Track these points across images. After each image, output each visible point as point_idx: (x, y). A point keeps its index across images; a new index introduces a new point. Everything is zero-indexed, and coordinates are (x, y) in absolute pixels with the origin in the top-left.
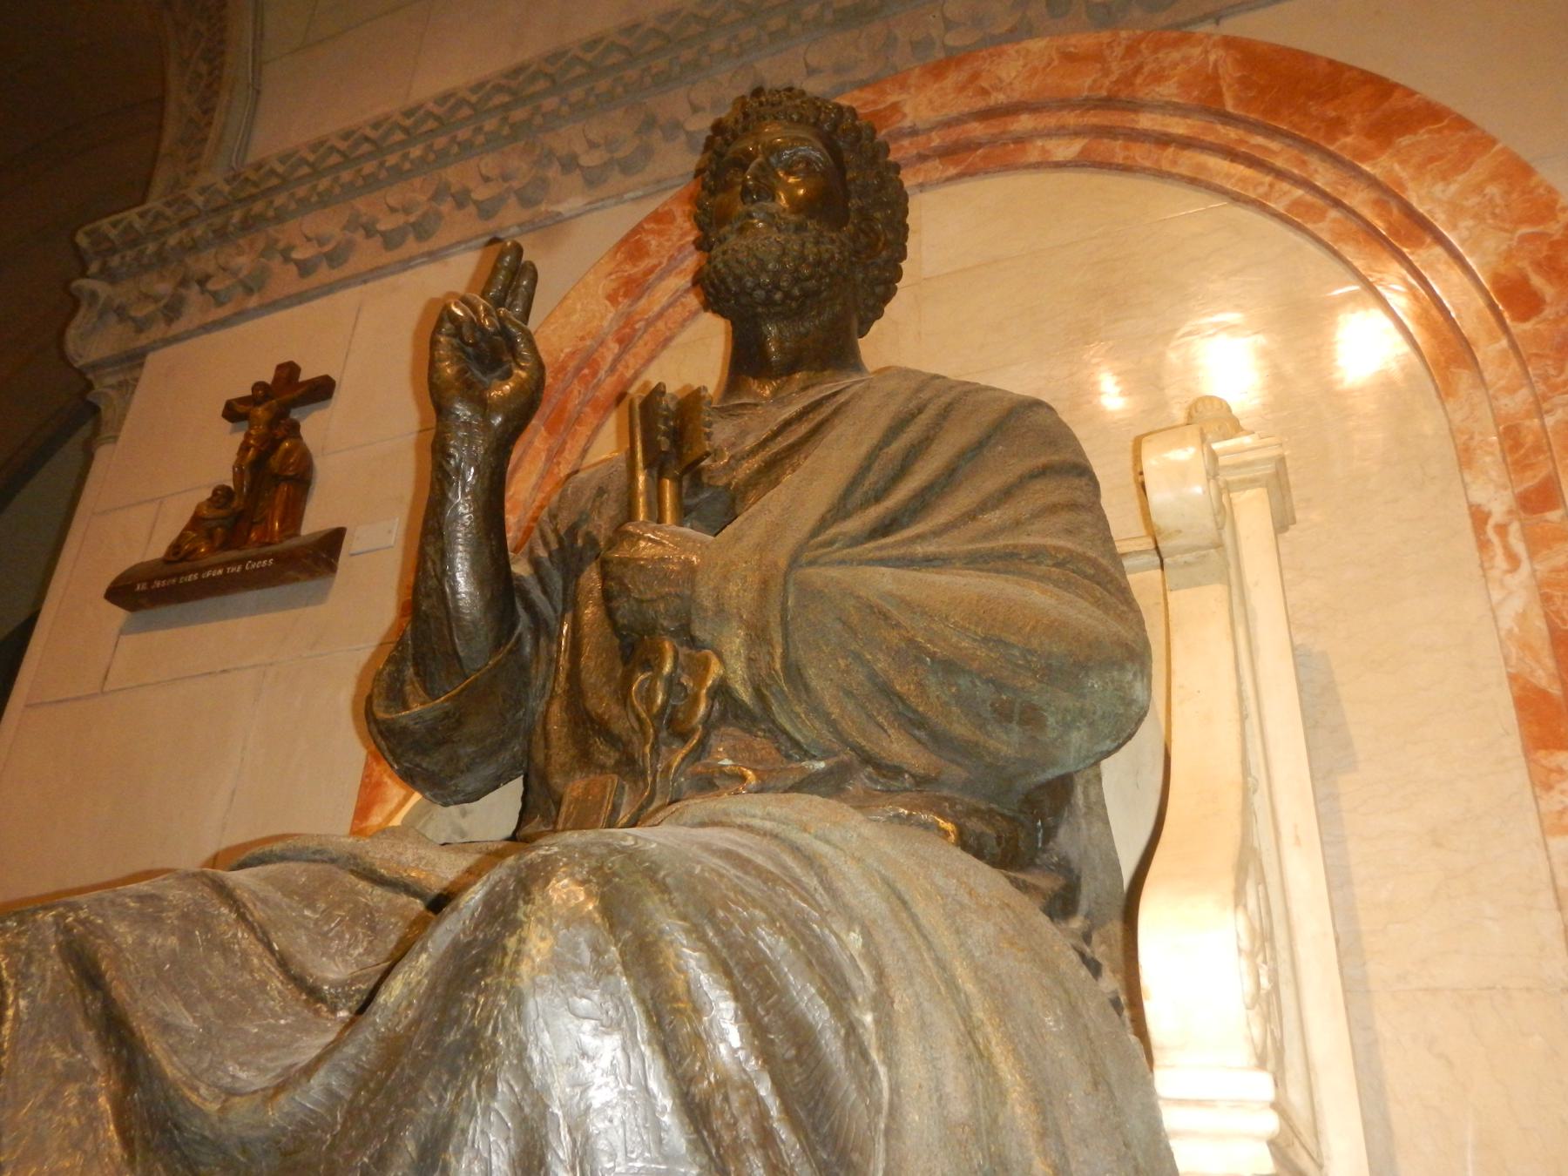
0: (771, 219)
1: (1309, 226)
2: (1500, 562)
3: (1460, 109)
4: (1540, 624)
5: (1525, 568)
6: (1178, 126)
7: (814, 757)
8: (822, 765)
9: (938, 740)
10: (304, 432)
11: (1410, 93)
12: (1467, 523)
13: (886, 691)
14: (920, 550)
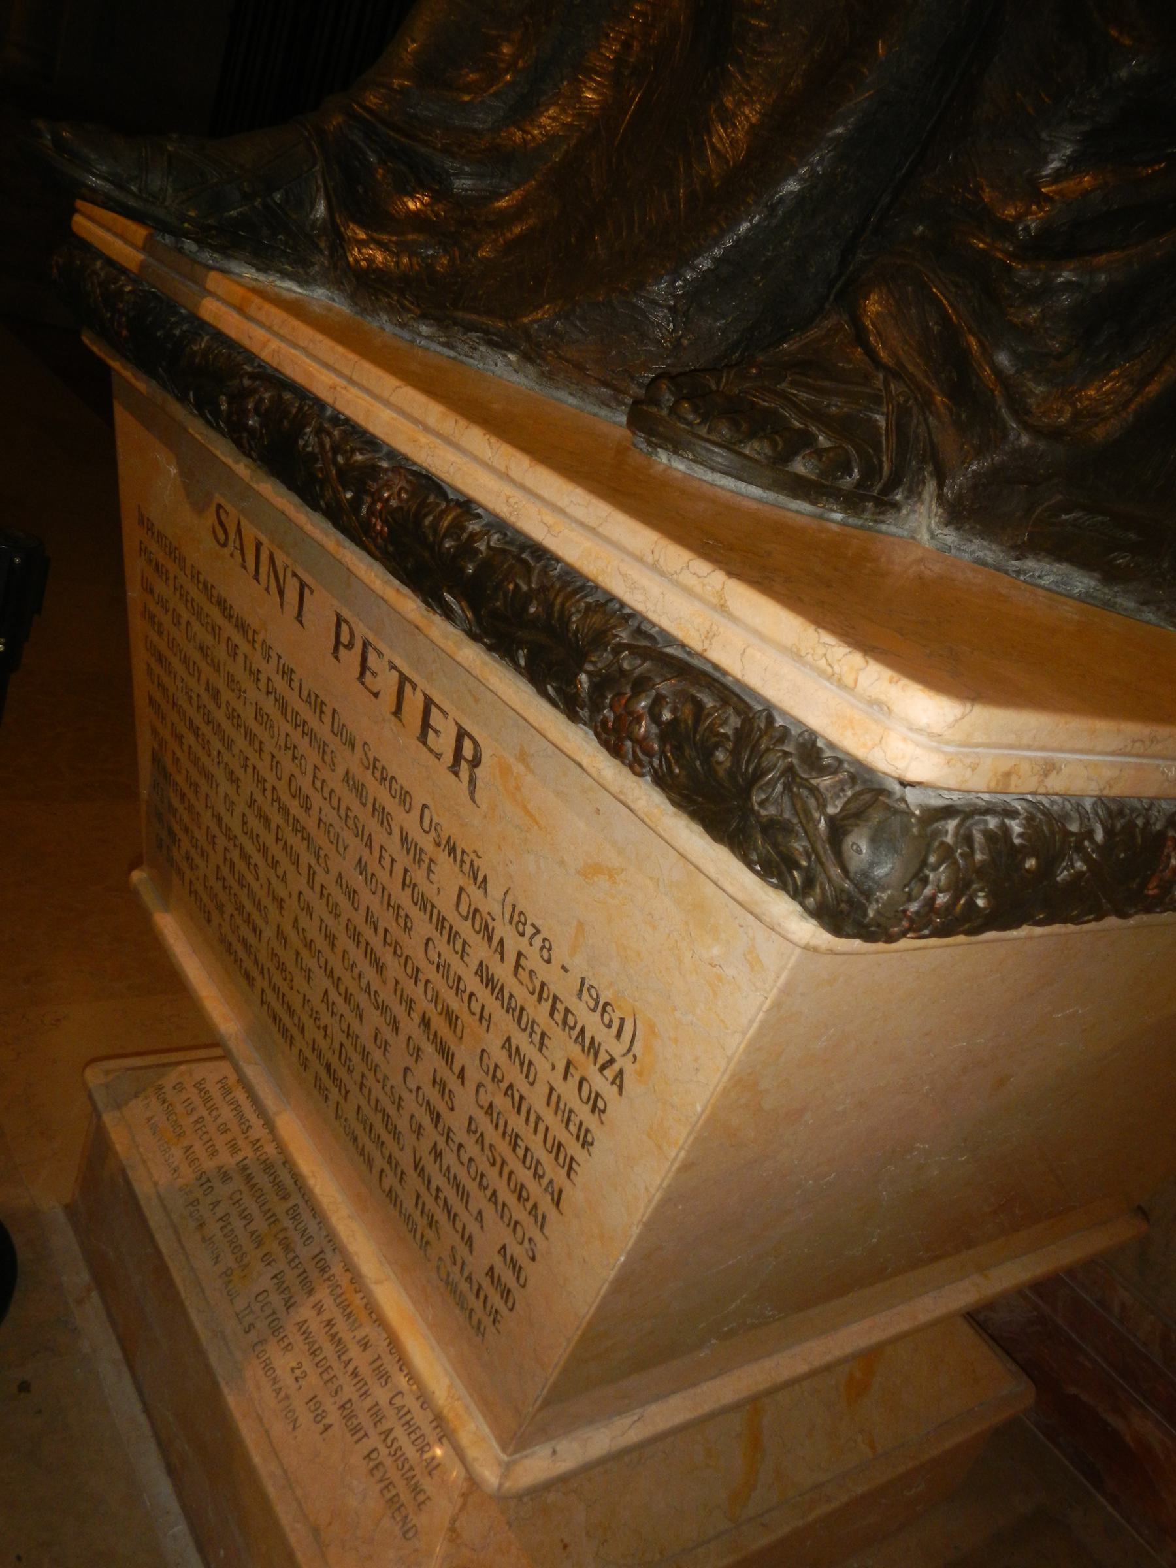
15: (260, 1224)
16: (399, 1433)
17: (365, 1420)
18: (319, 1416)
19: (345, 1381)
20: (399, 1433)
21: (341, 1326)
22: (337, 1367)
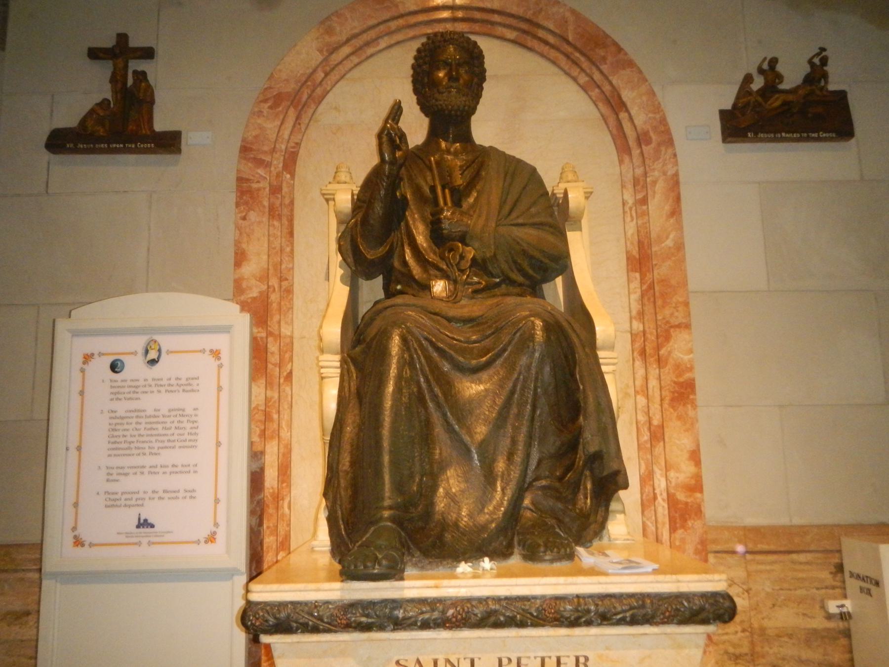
0: (459, 91)
1: (590, 93)
2: (628, 219)
3: (640, 65)
4: (636, 237)
6: (551, 39)
7: (495, 278)
8: (498, 280)
9: (525, 275)
10: (149, 78)
11: (626, 54)
12: (621, 204)
13: (515, 262)
14: (520, 221)
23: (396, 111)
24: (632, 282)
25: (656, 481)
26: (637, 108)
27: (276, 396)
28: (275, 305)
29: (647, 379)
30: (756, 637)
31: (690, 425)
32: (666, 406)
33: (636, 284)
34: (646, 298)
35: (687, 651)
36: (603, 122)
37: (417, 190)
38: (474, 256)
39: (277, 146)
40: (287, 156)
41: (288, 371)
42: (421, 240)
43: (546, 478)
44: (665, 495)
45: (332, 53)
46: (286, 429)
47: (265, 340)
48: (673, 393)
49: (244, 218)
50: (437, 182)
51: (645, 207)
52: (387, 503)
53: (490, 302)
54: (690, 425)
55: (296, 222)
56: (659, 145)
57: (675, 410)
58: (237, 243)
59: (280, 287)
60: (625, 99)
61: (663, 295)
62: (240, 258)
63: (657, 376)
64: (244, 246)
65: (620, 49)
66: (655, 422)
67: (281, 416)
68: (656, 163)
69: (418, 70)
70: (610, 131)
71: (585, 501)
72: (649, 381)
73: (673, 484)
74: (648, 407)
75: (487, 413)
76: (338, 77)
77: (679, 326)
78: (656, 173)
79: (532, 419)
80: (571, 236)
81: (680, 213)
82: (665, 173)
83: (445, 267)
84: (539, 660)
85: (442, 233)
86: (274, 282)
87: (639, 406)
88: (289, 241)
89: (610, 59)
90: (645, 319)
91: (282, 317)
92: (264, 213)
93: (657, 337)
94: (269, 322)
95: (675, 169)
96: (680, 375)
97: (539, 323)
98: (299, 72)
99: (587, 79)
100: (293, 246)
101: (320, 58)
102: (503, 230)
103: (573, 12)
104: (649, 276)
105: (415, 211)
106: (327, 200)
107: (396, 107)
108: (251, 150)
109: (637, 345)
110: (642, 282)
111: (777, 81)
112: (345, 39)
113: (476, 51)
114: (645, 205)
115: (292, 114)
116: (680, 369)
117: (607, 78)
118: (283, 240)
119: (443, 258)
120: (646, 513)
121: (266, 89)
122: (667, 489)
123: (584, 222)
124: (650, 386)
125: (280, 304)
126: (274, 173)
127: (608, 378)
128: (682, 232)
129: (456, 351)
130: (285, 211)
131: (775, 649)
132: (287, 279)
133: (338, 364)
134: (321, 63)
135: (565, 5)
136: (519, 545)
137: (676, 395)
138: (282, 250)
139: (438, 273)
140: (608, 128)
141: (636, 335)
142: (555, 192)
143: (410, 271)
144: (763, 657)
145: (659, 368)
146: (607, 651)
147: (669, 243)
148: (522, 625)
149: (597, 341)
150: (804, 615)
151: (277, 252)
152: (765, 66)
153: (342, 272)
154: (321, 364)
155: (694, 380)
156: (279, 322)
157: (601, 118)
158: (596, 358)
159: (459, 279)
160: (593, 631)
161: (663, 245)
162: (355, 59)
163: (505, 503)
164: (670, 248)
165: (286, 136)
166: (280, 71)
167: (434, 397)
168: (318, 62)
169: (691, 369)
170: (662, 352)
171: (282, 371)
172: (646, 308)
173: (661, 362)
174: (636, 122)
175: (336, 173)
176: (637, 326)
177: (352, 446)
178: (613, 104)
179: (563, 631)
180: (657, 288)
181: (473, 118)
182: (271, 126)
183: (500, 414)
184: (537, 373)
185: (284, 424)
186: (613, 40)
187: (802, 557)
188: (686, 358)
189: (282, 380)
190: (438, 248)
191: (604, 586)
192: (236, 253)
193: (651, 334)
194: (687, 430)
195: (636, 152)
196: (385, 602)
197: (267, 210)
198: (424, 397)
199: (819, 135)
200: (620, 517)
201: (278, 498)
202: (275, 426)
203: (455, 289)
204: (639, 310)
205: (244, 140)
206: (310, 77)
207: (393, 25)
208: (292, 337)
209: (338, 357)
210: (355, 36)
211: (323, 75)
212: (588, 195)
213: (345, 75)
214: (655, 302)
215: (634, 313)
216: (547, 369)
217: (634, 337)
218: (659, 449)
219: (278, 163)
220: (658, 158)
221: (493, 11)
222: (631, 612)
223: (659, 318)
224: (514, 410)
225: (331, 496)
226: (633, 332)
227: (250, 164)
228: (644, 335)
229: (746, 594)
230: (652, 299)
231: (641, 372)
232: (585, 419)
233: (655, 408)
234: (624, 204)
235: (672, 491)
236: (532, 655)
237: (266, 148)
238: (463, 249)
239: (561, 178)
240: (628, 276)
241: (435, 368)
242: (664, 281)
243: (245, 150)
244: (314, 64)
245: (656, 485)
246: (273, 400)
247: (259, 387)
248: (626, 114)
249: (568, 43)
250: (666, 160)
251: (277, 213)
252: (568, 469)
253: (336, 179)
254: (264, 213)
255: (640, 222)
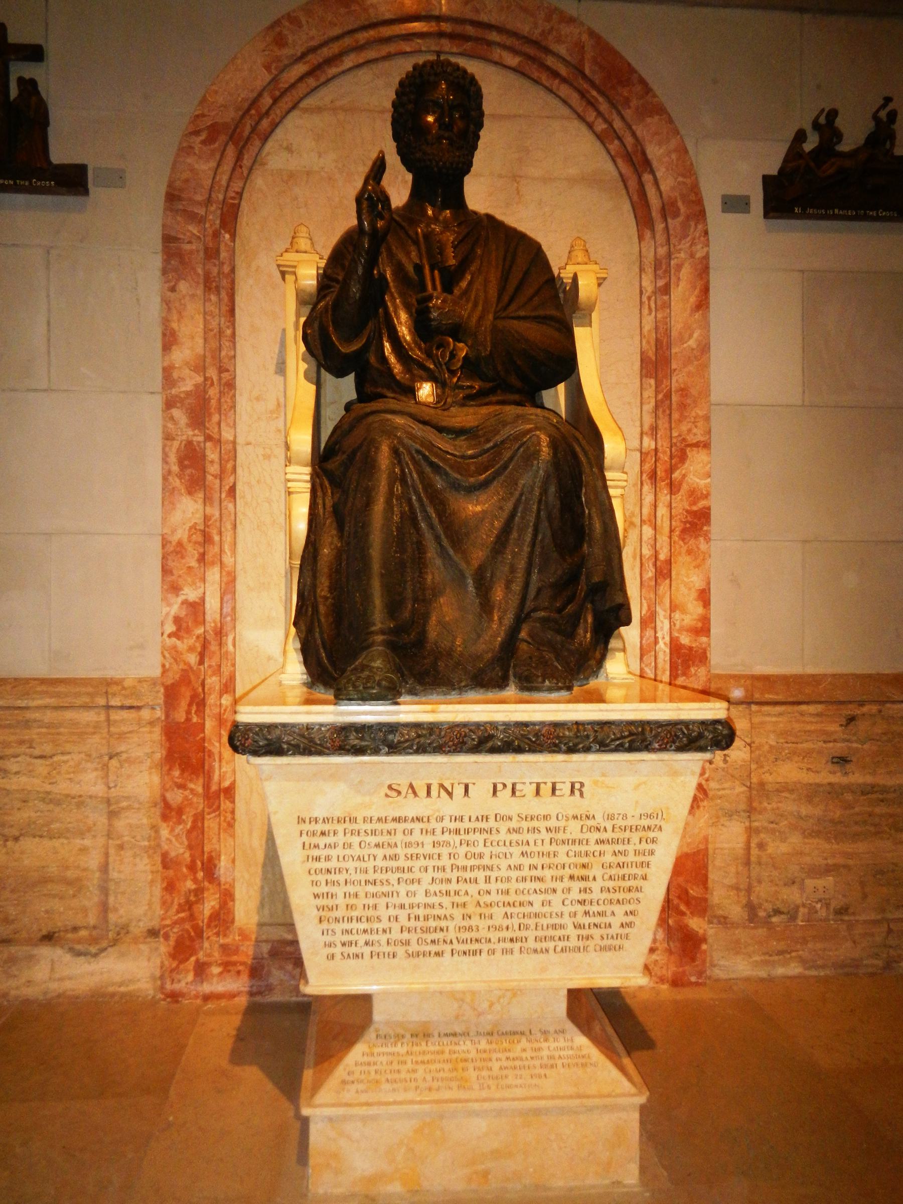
2: (645, 311)
5: (653, 313)
11: (655, 96)
14: (522, 313)
15: (447, 1067)
16: (562, 1053)
17: (552, 1062)
18: (540, 1076)
19: (532, 1063)
20: (562, 1053)
21: (511, 1055)
22: (526, 1063)
23: (379, 168)
24: (646, 389)
25: (658, 623)
26: (664, 170)
27: (217, 514)
28: (213, 403)
29: (655, 506)
30: (754, 792)
31: (699, 559)
32: (675, 538)
33: (650, 393)
34: (661, 410)
35: (682, 778)
36: (621, 183)
37: (399, 270)
38: (467, 354)
39: (213, 195)
40: (225, 209)
41: (231, 484)
42: (404, 332)
43: (545, 609)
44: (667, 639)
45: (282, 71)
46: (229, 554)
47: (202, 445)
48: (685, 523)
49: (173, 289)
50: (425, 261)
51: (666, 298)
52: (378, 626)
53: (484, 410)
54: (699, 559)
55: (238, 299)
56: (688, 218)
57: (685, 544)
58: (166, 322)
59: (220, 379)
60: (650, 157)
61: (683, 406)
62: (169, 340)
63: (667, 503)
64: (174, 325)
65: (647, 90)
66: (662, 557)
67: (224, 538)
68: (683, 242)
69: (401, 110)
70: (630, 198)
71: (585, 634)
72: (658, 509)
73: (678, 626)
74: (655, 539)
75: (484, 537)
76: (290, 105)
77: (696, 445)
78: (682, 255)
79: (533, 544)
80: (581, 334)
81: (708, 307)
82: (692, 256)
83: (432, 366)
84: (535, 785)
85: (431, 325)
86: (212, 373)
87: (645, 538)
88: (229, 321)
89: (634, 103)
90: (658, 436)
91: (223, 417)
92: (198, 283)
93: (671, 457)
94: (207, 425)
95: (705, 249)
96: (694, 503)
97: (544, 439)
98: (239, 95)
99: (605, 126)
100: (234, 329)
101: (268, 78)
102: (501, 324)
103: (592, 33)
104: (666, 383)
105: (396, 295)
106: (283, 274)
107: (378, 163)
108: (180, 199)
109: (647, 467)
110: (657, 392)
111: (835, 140)
112: (299, 54)
113: (473, 89)
114: (666, 294)
115: (231, 152)
116: (695, 495)
117: (629, 127)
118: (223, 320)
119: (429, 355)
120: (645, 658)
121: (197, 116)
122: (671, 632)
123: (594, 315)
124: (659, 514)
125: (219, 400)
126: (210, 231)
127: (616, 504)
128: (709, 331)
129: (452, 467)
130: (225, 283)
131: (774, 805)
132: (227, 371)
133: (308, 478)
134: (269, 83)
135: (582, 24)
136: (515, 676)
137: (688, 525)
138: (221, 332)
139: (422, 373)
140: (628, 192)
141: (647, 454)
142: (562, 275)
143: (390, 370)
144: (760, 813)
145: (671, 494)
146: (603, 778)
147: (692, 343)
148: (519, 750)
149: (606, 461)
150: (808, 769)
151: (215, 335)
152: (822, 120)
153: (306, 366)
154: (289, 476)
155: (709, 508)
156: (219, 424)
157: (620, 179)
158: (604, 479)
159: (448, 381)
160: (591, 757)
161: (685, 345)
162: (312, 82)
163: (502, 633)
164: (693, 349)
165: (224, 183)
166: (216, 92)
167: (428, 518)
168: (265, 84)
169: (707, 496)
170: (676, 475)
171: (223, 483)
172: (660, 422)
173: (673, 488)
174: (662, 188)
175: (293, 238)
176: (648, 443)
177: (331, 569)
178: (636, 162)
179: (560, 757)
180: (675, 398)
181: (467, 179)
182: (205, 167)
183: (498, 537)
184: (541, 494)
185: (226, 548)
186: (640, 76)
187: (812, 709)
188: (702, 483)
189: (223, 496)
190: (425, 343)
191: (605, 713)
192: (164, 335)
193: (665, 452)
194: (698, 567)
195: (660, 226)
196: (381, 726)
197: (201, 281)
198: (416, 517)
199: (877, 214)
200: (619, 655)
201: (221, 632)
202: (216, 549)
203: (444, 393)
204: (652, 425)
205: (170, 185)
206: (255, 102)
207: (362, 37)
208: (234, 443)
209: (308, 470)
210: (313, 50)
211: (270, 101)
212: (600, 282)
213: (299, 102)
214: (670, 415)
215: (646, 427)
216: (552, 489)
217: (644, 455)
218: (664, 587)
219: (214, 218)
220: (685, 236)
221: (489, 27)
222: (629, 739)
223: (675, 434)
224: (514, 535)
225: (303, 628)
226: (643, 450)
227: (179, 218)
228: (656, 454)
229: (748, 747)
230: (668, 412)
231: (649, 499)
232: (590, 546)
233: (663, 540)
234: (641, 293)
235: (676, 634)
236: (527, 781)
237: (199, 198)
238: (454, 345)
239: (569, 258)
240: (641, 380)
241: (428, 486)
242: (684, 391)
243: (172, 197)
244: (259, 84)
245: (658, 628)
246: (213, 519)
247: (196, 501)
248: (651, 177)
249: (584, 76)
250: (694, 239)
251: (214, 284)
252: (570, 600)
253: (292, 247)
254: (198, 283)
255: (659, 316)
